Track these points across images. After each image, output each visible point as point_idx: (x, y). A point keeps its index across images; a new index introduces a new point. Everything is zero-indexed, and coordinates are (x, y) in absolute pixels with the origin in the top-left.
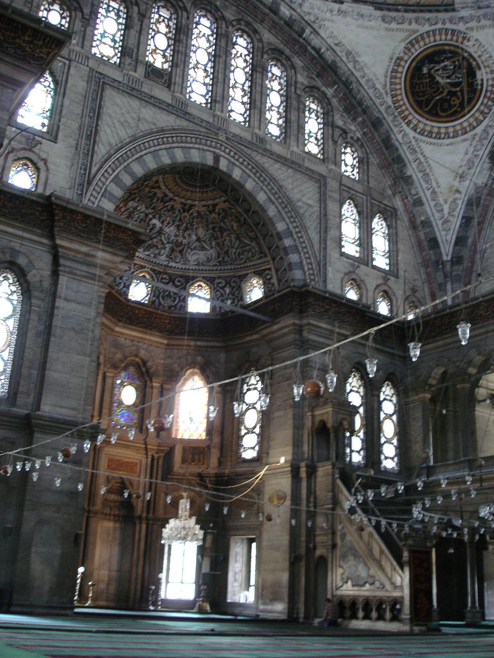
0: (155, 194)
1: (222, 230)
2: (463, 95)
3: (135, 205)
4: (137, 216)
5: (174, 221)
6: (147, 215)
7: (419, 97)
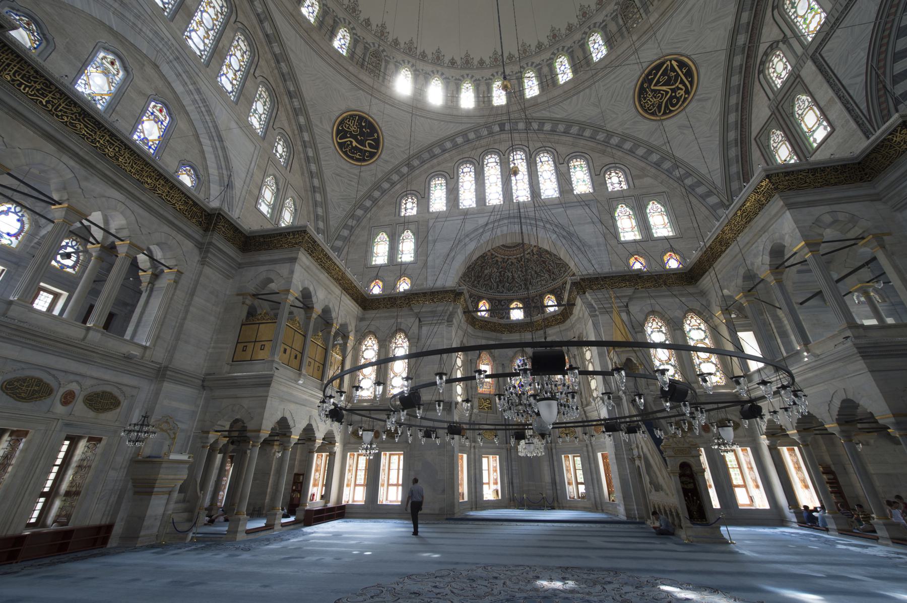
0: (497, 260)
1: (544, 262)
2: (685, 85)
5: (518, 269)
6: (500, 273)
7: (651, 110)
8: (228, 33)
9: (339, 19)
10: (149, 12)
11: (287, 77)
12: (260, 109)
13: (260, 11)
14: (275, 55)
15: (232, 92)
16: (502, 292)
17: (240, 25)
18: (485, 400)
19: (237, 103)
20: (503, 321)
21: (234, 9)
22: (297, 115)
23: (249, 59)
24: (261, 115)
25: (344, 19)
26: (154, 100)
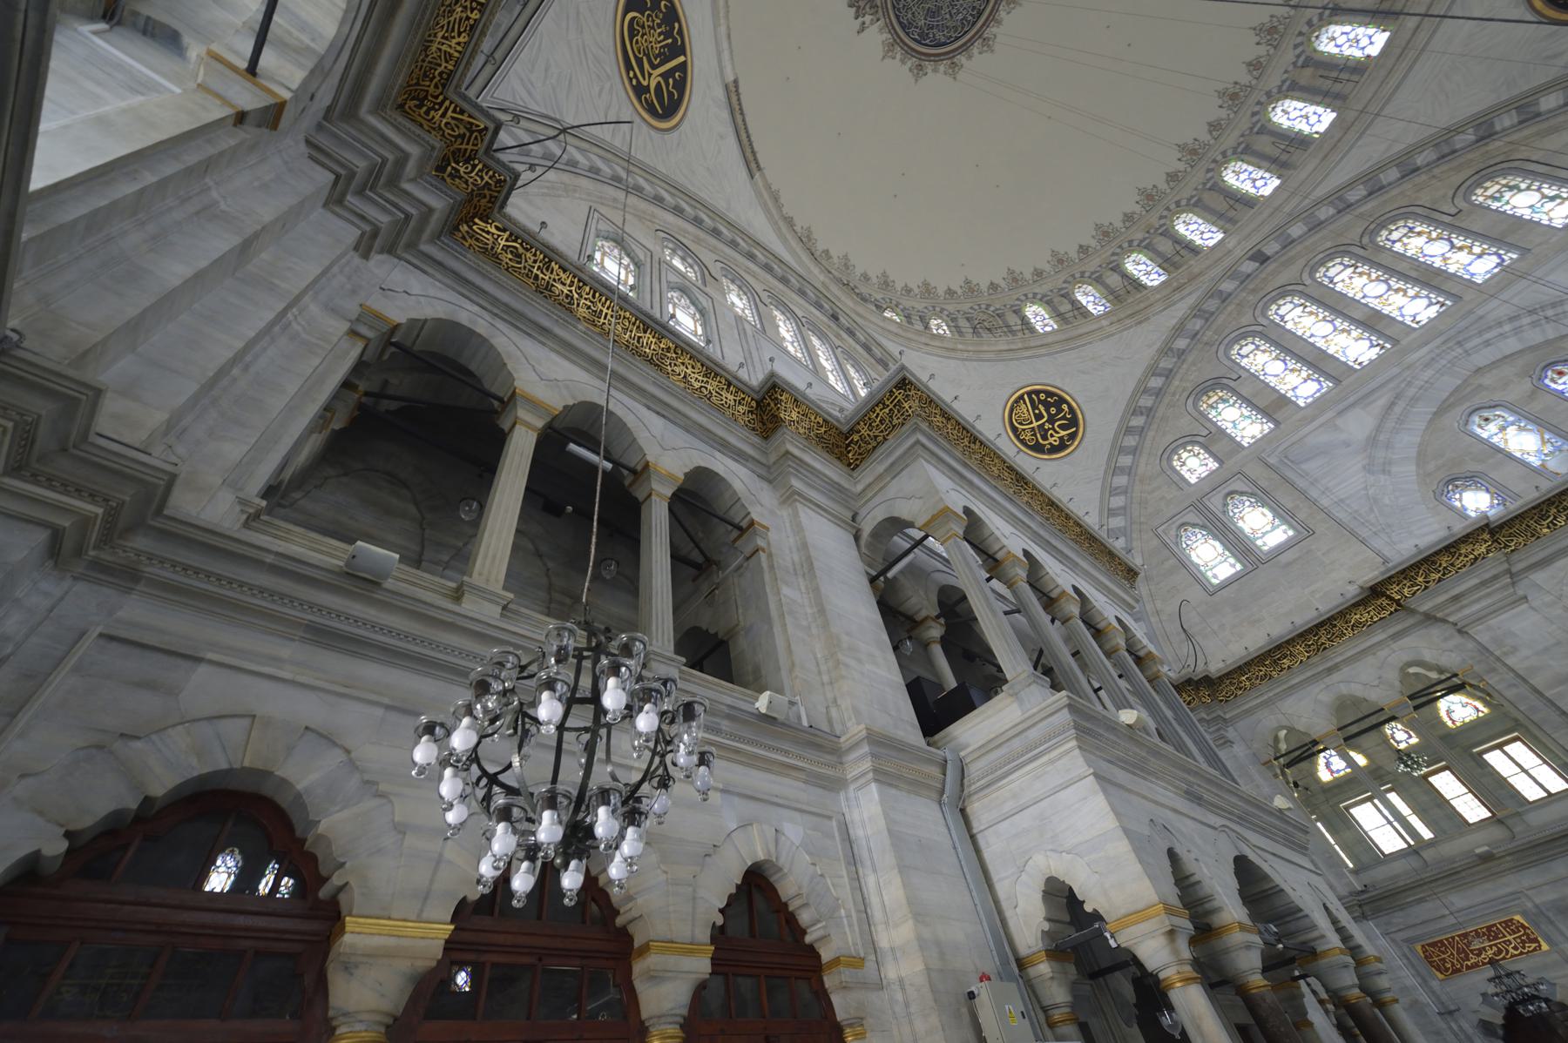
8: (1384, 259)
9: (1298, 56)
10: (1396, 370)
11: (1446, 150)
12: (1530, 198)
13: (1332, 211)
14: (1403, 177)
15: (1499, 256)
17: (1366, 240)
19: (1524, 251)
21: (1342, 248)
22: (1539, 115)
23: (1422, 223)
24: (1544, 196)
25: (1296, 46)
26: (1540, 379)
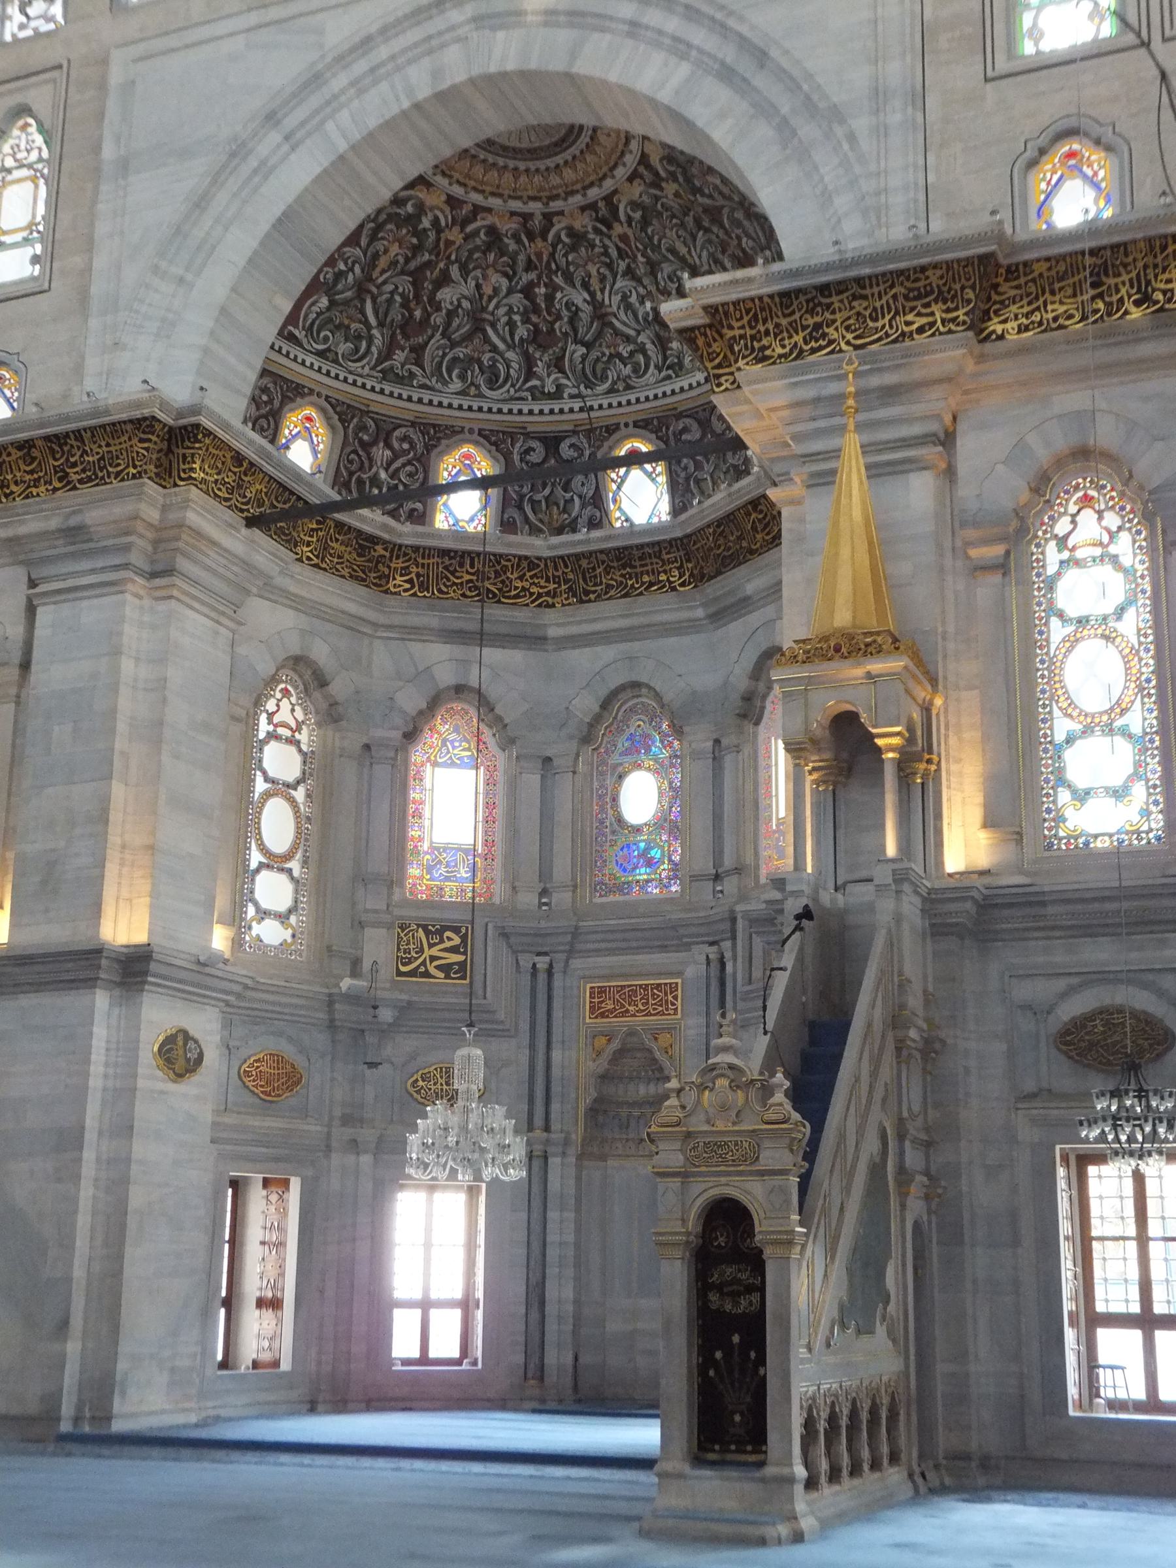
0: (492, 231)
3: (466, 289)
4: (502, 311)
5: (609, 266)
16: (557, 395)
18: (435, 932)
20: (582, 540)
